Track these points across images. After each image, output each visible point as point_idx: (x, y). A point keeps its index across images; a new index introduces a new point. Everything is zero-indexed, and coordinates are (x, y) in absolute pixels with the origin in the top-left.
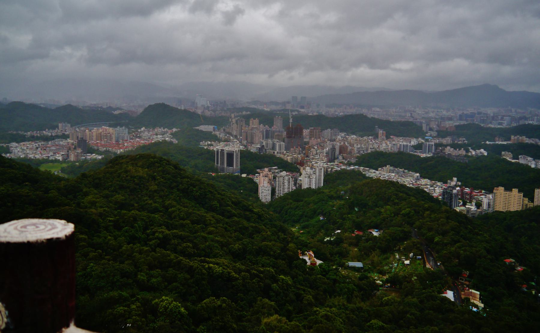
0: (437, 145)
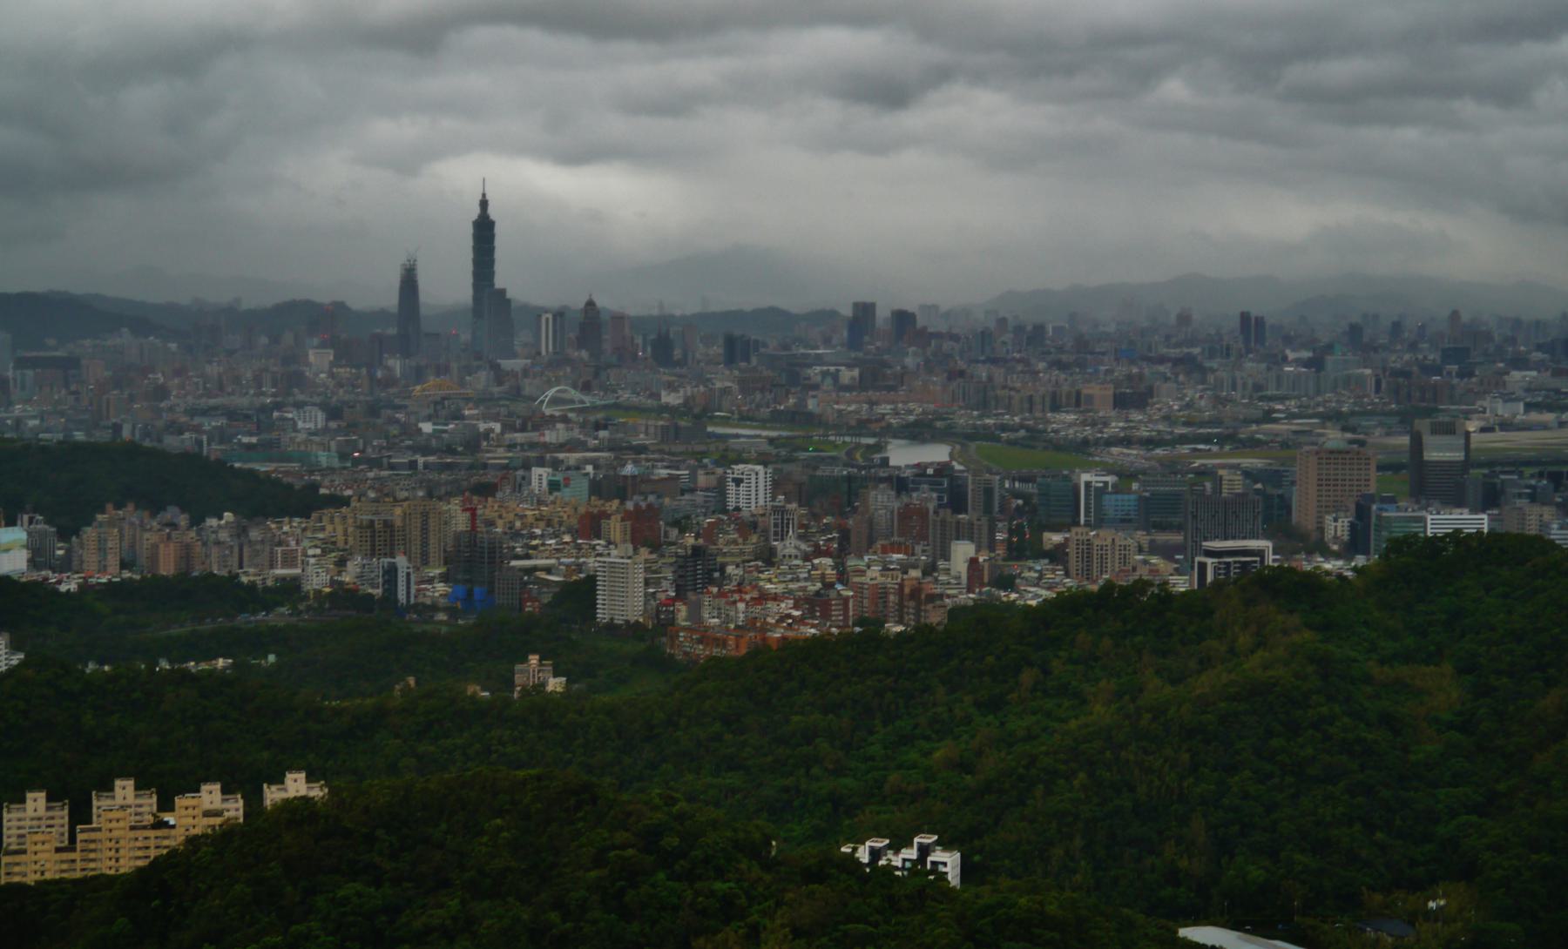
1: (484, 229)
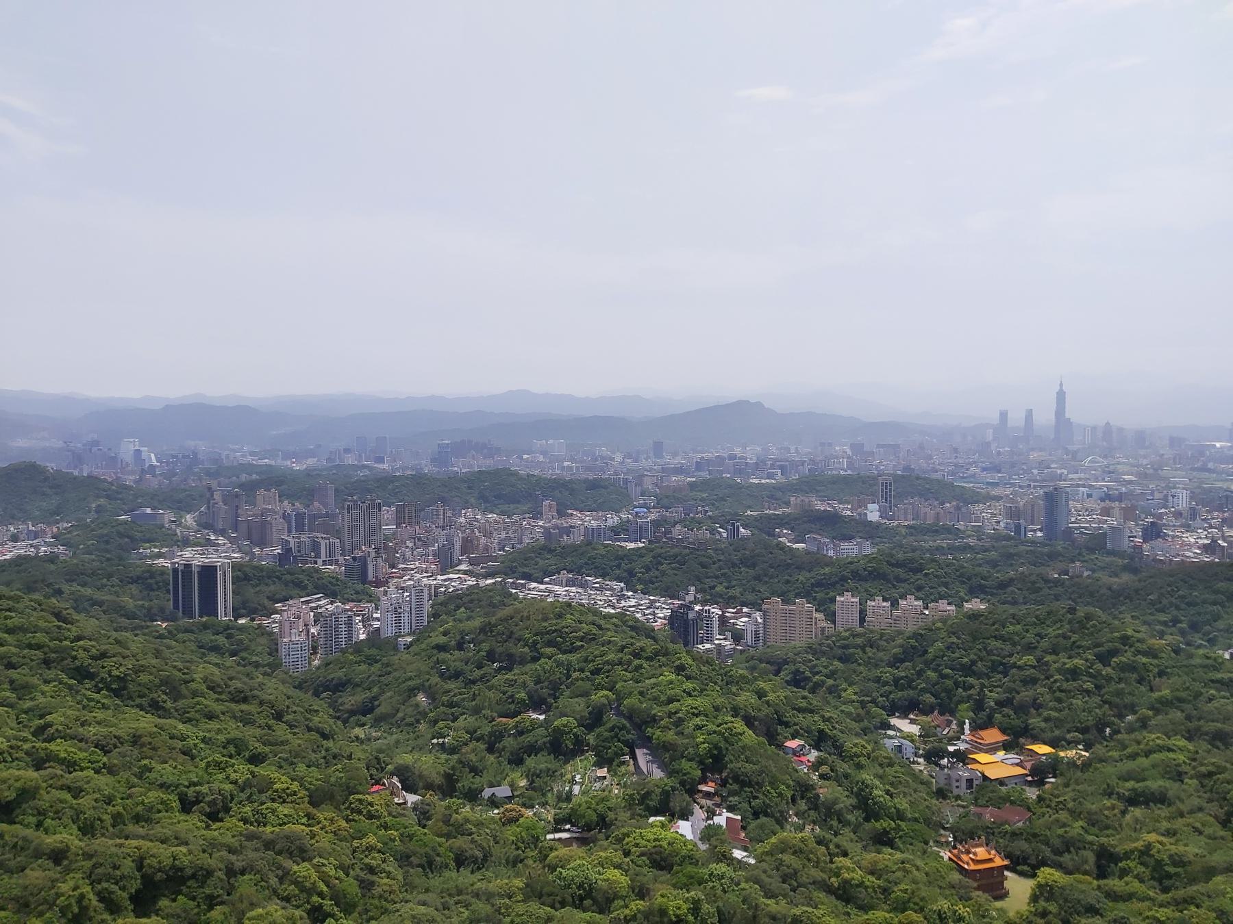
1: (1061, 396)
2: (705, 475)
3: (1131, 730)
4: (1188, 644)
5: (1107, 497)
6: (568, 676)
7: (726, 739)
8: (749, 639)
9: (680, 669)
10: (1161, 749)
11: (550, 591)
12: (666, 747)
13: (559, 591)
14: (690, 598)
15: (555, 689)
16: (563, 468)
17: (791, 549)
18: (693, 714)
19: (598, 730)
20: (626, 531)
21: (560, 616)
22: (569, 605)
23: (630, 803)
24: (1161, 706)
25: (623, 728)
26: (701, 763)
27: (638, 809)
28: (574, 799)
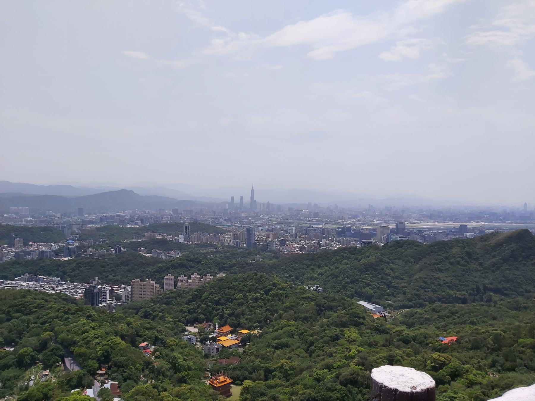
0: (78, 248)
1: (253, 191)
2: (105, 224)
3: (276, 320)
4: (295, 284)
5: (268, 230)
6: (28, 327)
7: (111, 347)
8: (124, 299)
9: (89, 317)
10: (286, 326)
11: (18, 285)
12: (81, 355)
13: (23, 284)
14: (95, 282)
15: (20, 335)
16: (27, 221)
17: (145, 256)
18: (96, 338)
19: (44, 352)
20: (62, 252)
21: (24, 297)
22: (29, 291)
23: (61, 385)
24: (288, 308)
25: (58, 349)
26: (99, 360)
27: (66, 388)
28: (30, 389)
